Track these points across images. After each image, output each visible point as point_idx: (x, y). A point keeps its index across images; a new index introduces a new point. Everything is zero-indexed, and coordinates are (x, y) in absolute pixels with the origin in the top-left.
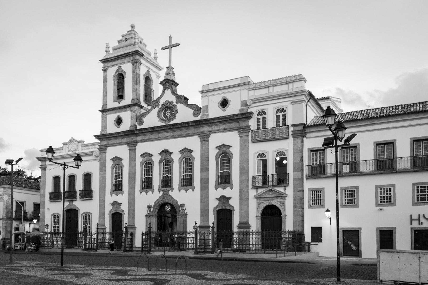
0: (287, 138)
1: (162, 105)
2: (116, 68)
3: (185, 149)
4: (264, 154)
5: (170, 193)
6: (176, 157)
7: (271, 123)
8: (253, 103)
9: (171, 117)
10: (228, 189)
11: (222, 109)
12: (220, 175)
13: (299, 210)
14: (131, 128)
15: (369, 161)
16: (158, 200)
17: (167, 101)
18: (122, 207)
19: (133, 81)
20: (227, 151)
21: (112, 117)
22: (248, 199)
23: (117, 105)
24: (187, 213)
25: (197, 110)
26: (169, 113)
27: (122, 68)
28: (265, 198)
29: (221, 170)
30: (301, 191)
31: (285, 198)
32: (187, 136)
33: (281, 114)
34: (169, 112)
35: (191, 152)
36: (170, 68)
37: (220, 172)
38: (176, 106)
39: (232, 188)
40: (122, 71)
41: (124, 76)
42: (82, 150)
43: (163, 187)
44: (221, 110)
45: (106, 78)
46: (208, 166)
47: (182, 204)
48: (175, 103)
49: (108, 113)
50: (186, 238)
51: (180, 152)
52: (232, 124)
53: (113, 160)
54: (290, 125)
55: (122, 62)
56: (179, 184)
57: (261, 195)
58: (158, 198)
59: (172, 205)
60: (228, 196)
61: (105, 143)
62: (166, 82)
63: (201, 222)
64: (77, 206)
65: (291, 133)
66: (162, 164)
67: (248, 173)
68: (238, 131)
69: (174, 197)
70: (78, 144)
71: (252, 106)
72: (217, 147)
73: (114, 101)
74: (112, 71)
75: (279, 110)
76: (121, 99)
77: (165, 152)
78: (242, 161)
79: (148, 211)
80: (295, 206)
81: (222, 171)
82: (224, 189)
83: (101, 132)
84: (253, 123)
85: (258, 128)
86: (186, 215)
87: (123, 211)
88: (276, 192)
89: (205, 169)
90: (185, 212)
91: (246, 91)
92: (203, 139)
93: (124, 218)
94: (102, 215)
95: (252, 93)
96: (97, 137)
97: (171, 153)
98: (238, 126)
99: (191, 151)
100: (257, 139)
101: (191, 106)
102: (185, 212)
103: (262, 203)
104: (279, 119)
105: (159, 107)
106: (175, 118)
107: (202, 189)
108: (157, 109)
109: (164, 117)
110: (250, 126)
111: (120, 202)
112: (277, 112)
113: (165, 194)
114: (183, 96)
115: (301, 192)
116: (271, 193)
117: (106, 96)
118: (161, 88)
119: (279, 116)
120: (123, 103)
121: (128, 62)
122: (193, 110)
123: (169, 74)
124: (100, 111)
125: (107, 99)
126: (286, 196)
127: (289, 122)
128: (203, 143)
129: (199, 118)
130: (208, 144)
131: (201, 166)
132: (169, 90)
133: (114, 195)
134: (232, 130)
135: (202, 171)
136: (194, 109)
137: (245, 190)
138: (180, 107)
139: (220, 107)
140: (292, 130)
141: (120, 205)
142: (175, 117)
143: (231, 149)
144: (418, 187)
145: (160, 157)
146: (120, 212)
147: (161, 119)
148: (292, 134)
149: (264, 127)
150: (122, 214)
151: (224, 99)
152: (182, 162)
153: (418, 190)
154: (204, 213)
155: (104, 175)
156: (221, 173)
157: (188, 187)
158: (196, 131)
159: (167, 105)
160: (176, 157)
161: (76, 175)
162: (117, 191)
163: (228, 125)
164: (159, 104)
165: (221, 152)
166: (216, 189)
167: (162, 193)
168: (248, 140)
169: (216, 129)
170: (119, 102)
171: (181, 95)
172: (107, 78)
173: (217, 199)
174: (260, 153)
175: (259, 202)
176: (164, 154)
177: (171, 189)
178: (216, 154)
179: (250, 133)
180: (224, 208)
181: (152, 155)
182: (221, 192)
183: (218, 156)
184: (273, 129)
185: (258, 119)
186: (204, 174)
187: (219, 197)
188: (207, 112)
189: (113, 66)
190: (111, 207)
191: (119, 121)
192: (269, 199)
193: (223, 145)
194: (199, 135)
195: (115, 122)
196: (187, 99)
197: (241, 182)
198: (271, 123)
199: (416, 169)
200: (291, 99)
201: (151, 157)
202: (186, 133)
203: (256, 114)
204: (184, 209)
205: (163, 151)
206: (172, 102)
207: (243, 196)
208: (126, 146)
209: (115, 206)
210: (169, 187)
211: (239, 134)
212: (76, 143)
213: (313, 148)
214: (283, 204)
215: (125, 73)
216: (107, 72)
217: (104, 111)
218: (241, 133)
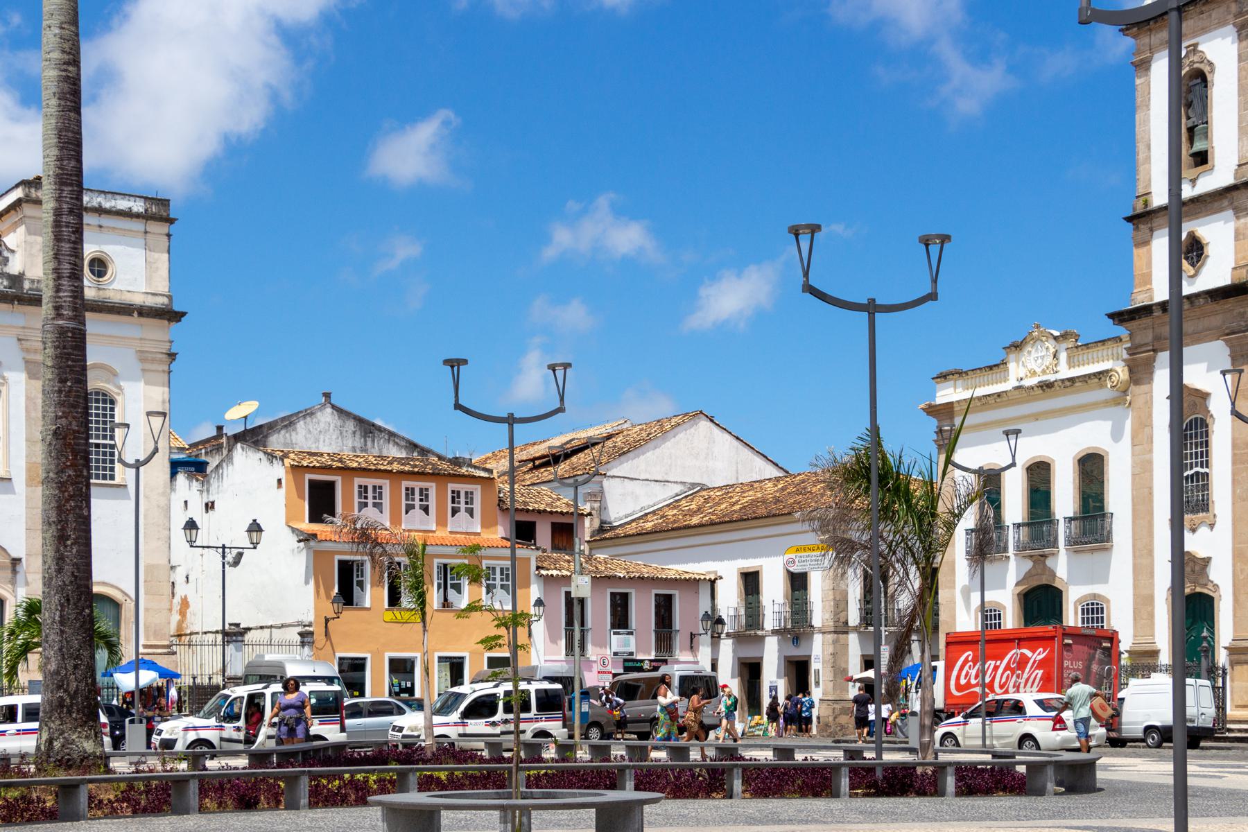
14: (1235, 272)
19: (1239, 96)
41: (1209, 79)
45: (1146, 93)
121: (1222, 23)
155: (1147, 457)
172: (1149, 93)
191: (1192, 251)
215: (1211, 64)
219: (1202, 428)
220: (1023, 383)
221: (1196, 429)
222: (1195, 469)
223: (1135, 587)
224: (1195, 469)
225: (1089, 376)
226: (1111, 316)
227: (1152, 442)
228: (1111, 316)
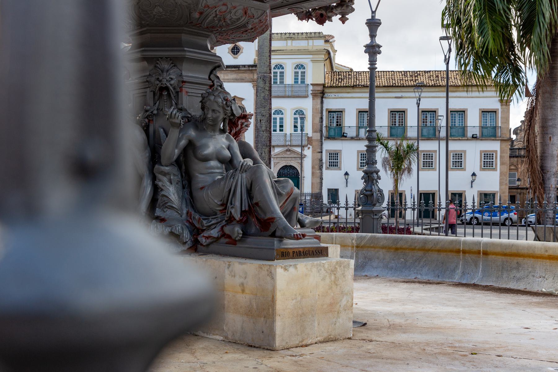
0: (306, 97)
4: (281, 111)
11: (233, 57)
13: (318, 171)
15: (384, 127)
28: (282, 157)
30: (319, 152)
33: (300, 71)
44: (233, 58)
52: (244, 74)
54: (309, 84)
57: (278, 154)
65: (310, 92)
68: (252, 84)
75: (297, 66)
80: (313, 168)
88: (294, 152)
103: (278, 163)
104: (298, 76)
112: (295, 68)
115: (320, 154)
116: (288, 153)
119: (298, 72)
126: (305, 157)
127: (309, 80)
134: (245, 81)
139: (231, 52)
140: (312, 89)
144: (424, 154)
148: (311, 94)
163: (240, 75)
174: (277, 109)
175: (275, 161)
184: (291, 86)
192: (286, 159)
199: (423, 138)
200: (311, 56)
213: (331, 109)
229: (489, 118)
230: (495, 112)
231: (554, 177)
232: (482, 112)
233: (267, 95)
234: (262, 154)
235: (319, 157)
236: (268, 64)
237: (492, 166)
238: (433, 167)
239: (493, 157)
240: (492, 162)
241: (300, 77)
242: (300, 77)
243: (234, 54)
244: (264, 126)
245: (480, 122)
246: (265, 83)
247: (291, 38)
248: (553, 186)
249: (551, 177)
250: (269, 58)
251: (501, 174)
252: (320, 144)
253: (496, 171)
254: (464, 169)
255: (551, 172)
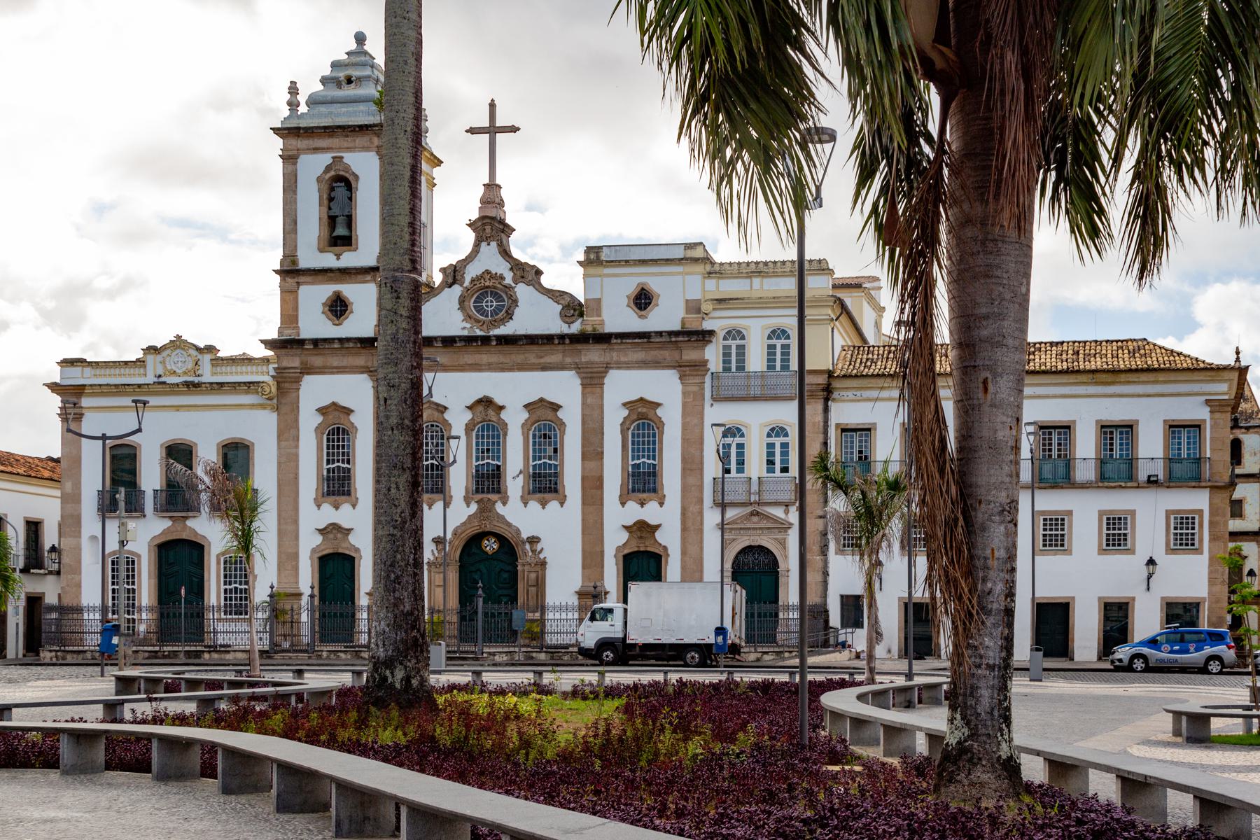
1: (473, 281)
2: (325, 159)
3: (542, 400)
4: (739, 430)
5: (499, 508)
6: (515, 418)
7: (756, 361)
8: (714, 309)
9: (497, 314)
10: (653, 506)
12: (630, 469)
16: (464, 524)
17: (488, 272)
18: (352, 539)
20: (651, 415)
21: (314, 296)
22: (700, 531)
23: (329, 260)
24: (547, 560)
25: (572, 308)
26: (489, 304)
27: (345, 160)
29: (633, 460)
30: (821, 517)
31: (786, 531)
32: (544, 368)
33: (779, 343)
34: (492, 302)
35: (557, 410)
36: (492, 188)
37: (631, 463)
38: (513, 288)
39: (661, 504)
40: (347, 168)
42: (213, 374)
43: (477, 491)
46: (602, 447)
47: (533, 537)
48: (509, 280)
49: (302, 279)
50: (542, 622)
51: (526, 406)
52: (662, 352)
53: (322, 411)
55: (346, 145)
56: (523, 487)
58: (464, 519)
59: (500, 538)
60: (652, 522)
61: (295, 362)
62: (484, 224)
63: (583, 582)
64: (199, 532)
66: (474, 434)
67: (702, 469)
69: (509, 519)
70: (200, 357)
71: (710, 316)
72: (624, 405)
73: (321, 250)
74: (314, 165)
75: (774, 332)
76: (345, 248)
77: (486, 402)
78: (685, 440)
79: (436, 552)
81: (638, 462)
82: (642, 504)
83: (280, 331)
84: (713, 355)
85: (727, 369)
86: (543, 564)
87: (357, 550)
88: (768, 517)
89: (593, 451)
90: (542, 556)
91: (698, 278)
92: (588, 381)
93: (361, 569)
94: (288, 559)
95: (711, 284)
96: (268, 344)
97: (502, 408)
98: (678, 358)
99: (556, 407)
100: (723, 393)
101: (556, 295)
102: (542, 556)
103: (734, 540)
104: (775, 354)
105: (465, 285)
106: (511, 318)
107: (586, 501)
108: (457, 290)
109: (478, 312)
110: (708, 361)
111: (346, 525)
112: (769, 338)
113: (486, 509)
114: (534, 266)
115: (821, 521)
116: (755, 519)
117: (295, 231)
118: (469, 237)
120: (349, 259)
121: (366, 149)
122: (560, 307)
123: (494, 202)
124: (276, 272)
125: (296, 239)
128: (588, 390)
129: (575, 328)
130: (603, 392)
131: (583, 446)
132: (494, 244)
133: (327, 507)
135: (584, 457)
136: (563, 302)
137: (693, 508)
138: (522, 291)
139: (632, 305)
141: (348, 534)
142: (509, 316)
143: (659, 412)
144: (1045, 520)
145: (468, 416)
146: (347, 552)
147: (468, 317)
149: (741, 368)
150: (353, 558)
151: (643, 289)
152: (531, 433)
153: (1045, 525)
154: (592, 558)
155: (294, 451)
156: (633, 466)
157: (547, 496)
158: (568, 360)
159: (487, 284)
160: (515, 418)
161: (196, 444)
162: (334, 495)
164: (463, 276)
165: (635, 417)
166: (623, 504)
167: (474, 507)
168: (703, 395)
169: (623, 359)
170: (338, 256)
171: (526, 263)
172: (296, 182)
173: (626, 527)
176: (480, 408)
177: (500, 498)
178: (622, 420)
179: (708, 379)
180: (642, 549)
181: (446, 408)
182: (634, 512)
183: (627, 425)
184: (762, 375)
185: (725, 347)
186: (592, 464)
187: (630, 522)
188: (599, 315)
189: (316, 150)
190: (318, 539)
191: (338, 307)
193: (641, 399)
194: (578, 368)
195: (327, 308)
196: (539, 273)
197: (685, 489)
198: (756, 361)
199: (1042, 485)
201: (443, 413)
202: (542, 361)
203: (721, 334)
204: (539, 549)
205: (479, 401)
206: (502, 278)
207: (689, 524)
208: (365, 376)
209: (331, 536)
210: (493, 492)
211: (680, 378)
212: (194, 353)
214: (783, 544)
215: (357, 177)
216: (295, 164)
217: (291, 272)
218: (685, 375)
219: (343, 434)
220: (162, 379)
221: (338, 434)
222: (336, 464)
223: (280, 546)
224: (336, 464)
225: (239, 383)
226: (262, 341)
227: (298, 440)
228: (264, 342)
229: (1184, 441)
230: (1199, 426)
231: (1002, 522)
232: (1171, 426)
233: (405, 329)
234: (389, 490)
235: (821, 528)
236: (406, 245)
237: (1193, 545)
238: (1066, 547)
239: (1193, 523)
240: (1193, 534)
241: (778, 357)
242: (778, 357)
243: (640, 309)
244: (395, 414)
245: (1166, 448)
246: (398, 298)
247: (760, 272)
248: (996, 554)
249: (991, 521)
250: (410, 230)
251: (1211, 559)
252: (822, 500)
253: (1202, 553)
254: (1131, 551)
255: (989, 503)
